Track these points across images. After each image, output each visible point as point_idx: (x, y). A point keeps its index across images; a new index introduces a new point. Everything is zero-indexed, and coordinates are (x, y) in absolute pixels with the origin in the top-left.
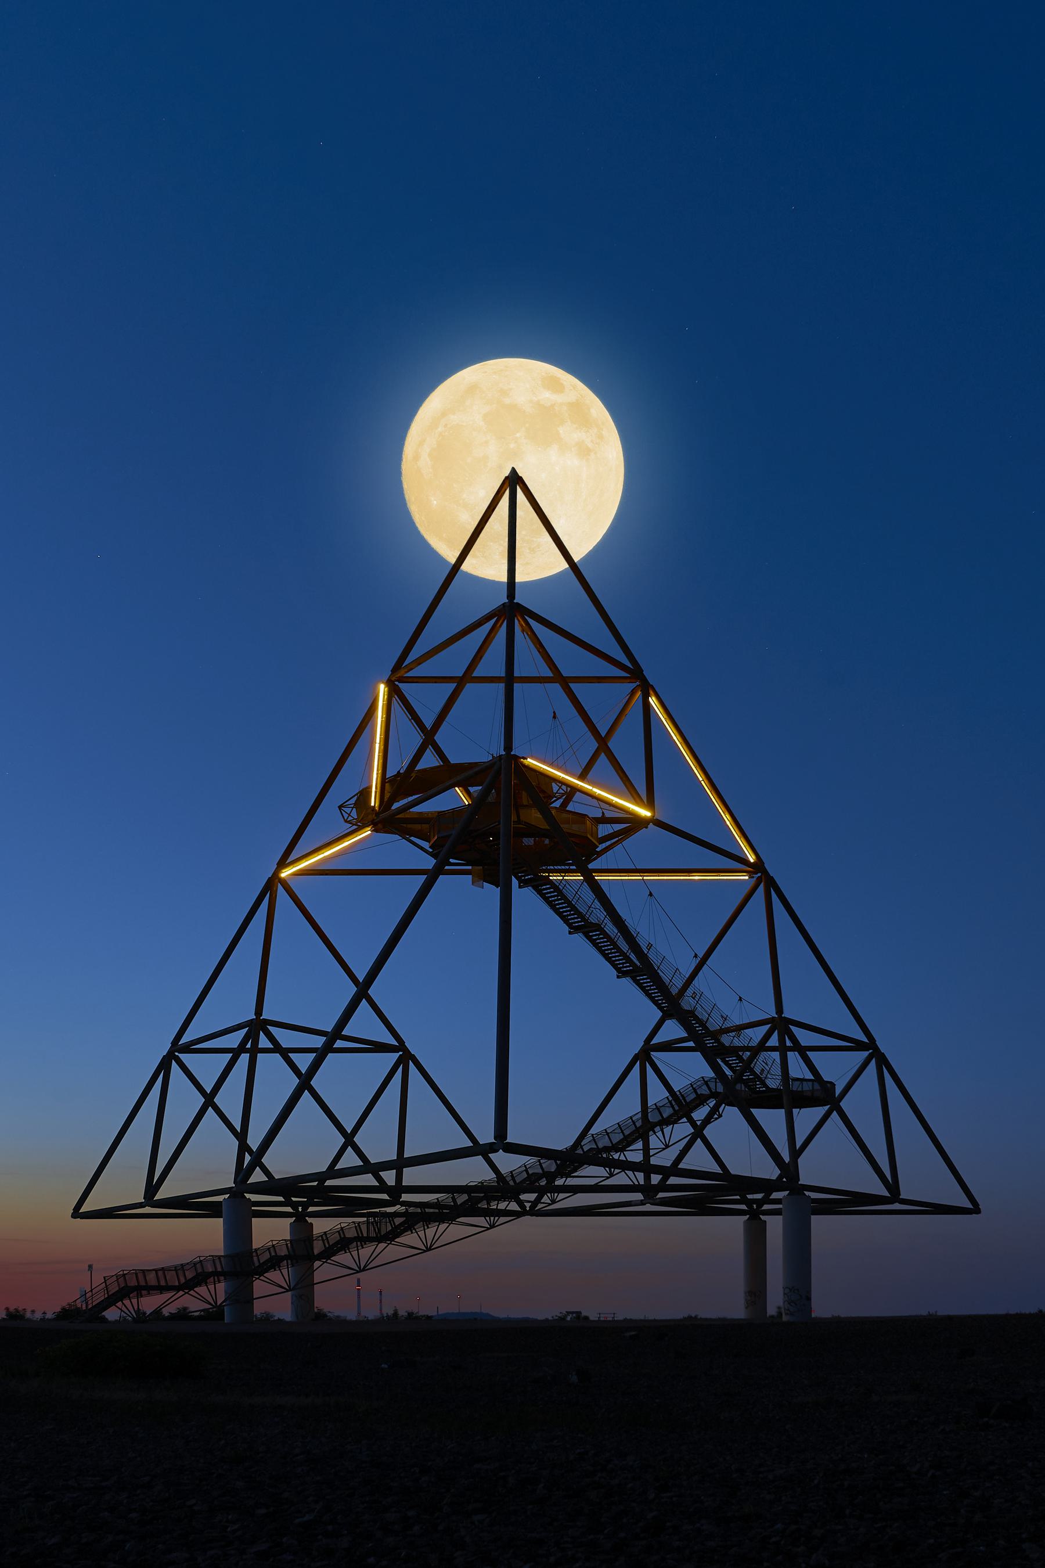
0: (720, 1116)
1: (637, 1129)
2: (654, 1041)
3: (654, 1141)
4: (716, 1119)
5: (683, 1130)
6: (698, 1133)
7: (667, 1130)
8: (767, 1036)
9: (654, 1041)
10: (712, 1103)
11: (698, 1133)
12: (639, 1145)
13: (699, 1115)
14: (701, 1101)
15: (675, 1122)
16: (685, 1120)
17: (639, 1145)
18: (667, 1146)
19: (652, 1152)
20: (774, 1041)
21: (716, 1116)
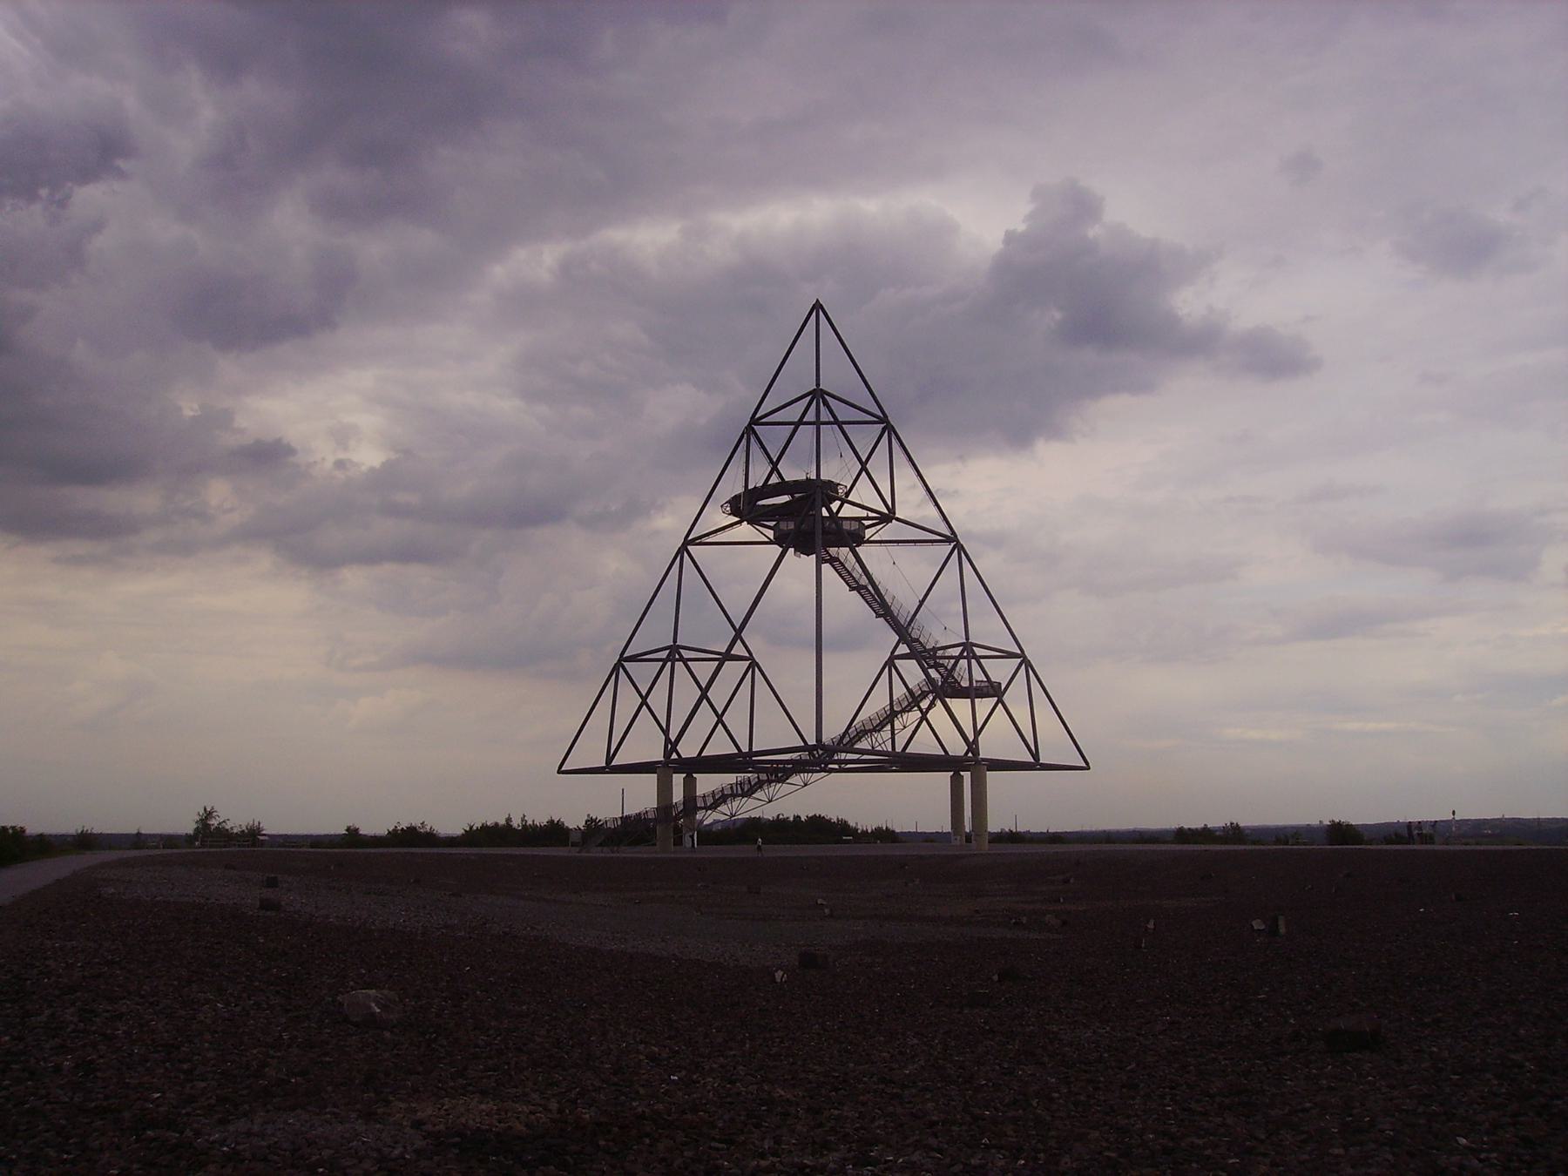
1: (888, 716)
2: (896, 653)
3: (897, 724)
5: (915, 715)
6: (924, 718)
7: (905, 716)
8: (962, 652)
9: (896, 653)
11: (924, 718)
12: (889, 727)
13: (924, 704)
14: (924, 695)
16: (916, 708)
17: (889, 727)
18: (905, 727)
19: (896, 732)
20: (965, 654)
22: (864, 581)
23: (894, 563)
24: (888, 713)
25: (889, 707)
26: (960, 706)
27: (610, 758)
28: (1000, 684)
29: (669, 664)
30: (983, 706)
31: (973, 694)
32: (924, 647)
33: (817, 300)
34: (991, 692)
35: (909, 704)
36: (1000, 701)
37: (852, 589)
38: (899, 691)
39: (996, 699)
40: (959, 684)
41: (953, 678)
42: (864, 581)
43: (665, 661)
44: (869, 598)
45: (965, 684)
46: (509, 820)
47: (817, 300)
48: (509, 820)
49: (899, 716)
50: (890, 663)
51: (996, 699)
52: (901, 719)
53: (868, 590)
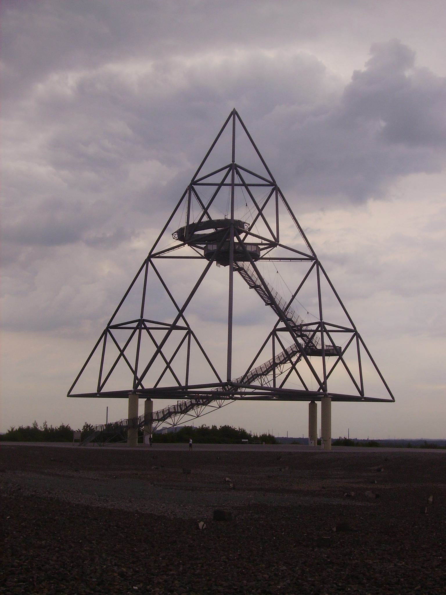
0: (301, 360)
3: (277, 371)
4: (299, 361)
5: (288, 365)
6: (294, 367)
7: (282, 366)
8: (318, 328)
10: (298, 355)
11: (294, 367)
12: (272, 373)
13: (294, 359)
14: (294, 353)
15: (285, 363)
16: (289, 361)
17: (272, 373)
18: (282, 373)
19: (276, 376)
20: (320, 329)
21: (299, 360)
22: (259, 282)
23: (277, 272)
24: (272, 364)
25: (272, 360)
26: (316, 361)
27: (100, 388)
28: (340, 348)
29: (138, 330)
30: (331, 361)
31: (324, 354)
32: (295, 324)
33: (234, 108)
34: (335, 352)
35: (285, 359)
36: (341, 358)
37: (251, 287)
38: (279, 351)
39: (338, 357)
40: (316, 347)
41: (312, 343)
42: (259, 282)
43: (135, 329)
44: (262, 293)
45: (319, 347)
46: (86, 423)
47: (234, 108)
48: (86, 423)
49: (278, 366)
50: (274, 333)
51: (338, 357)
52: (279, 368)
53: (261, 288)
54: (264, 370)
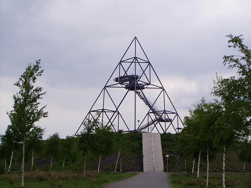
3: (149, 127)
5: (153, 125)
7: (151, 125)
11: (155, 126)
12: (148, 128)
13: (155, 123)
14: (155, 121)
17: (148, 128)
22: (144, 97)
26: (163, 124)
30: (168, 124)
31: (165, 121)
36: (171, 123)
37: (141, 99)
38: (150, 120)
42: (144, 97)
45: (164, 119)
50: (148, 114)
54: (145, 127)
